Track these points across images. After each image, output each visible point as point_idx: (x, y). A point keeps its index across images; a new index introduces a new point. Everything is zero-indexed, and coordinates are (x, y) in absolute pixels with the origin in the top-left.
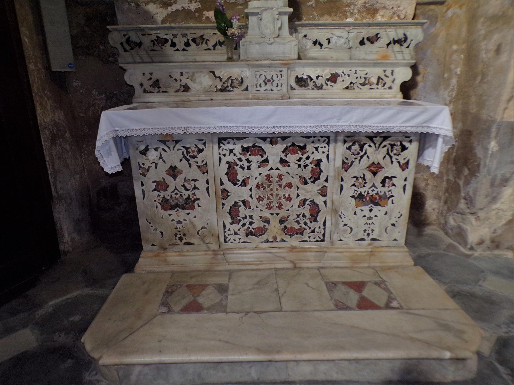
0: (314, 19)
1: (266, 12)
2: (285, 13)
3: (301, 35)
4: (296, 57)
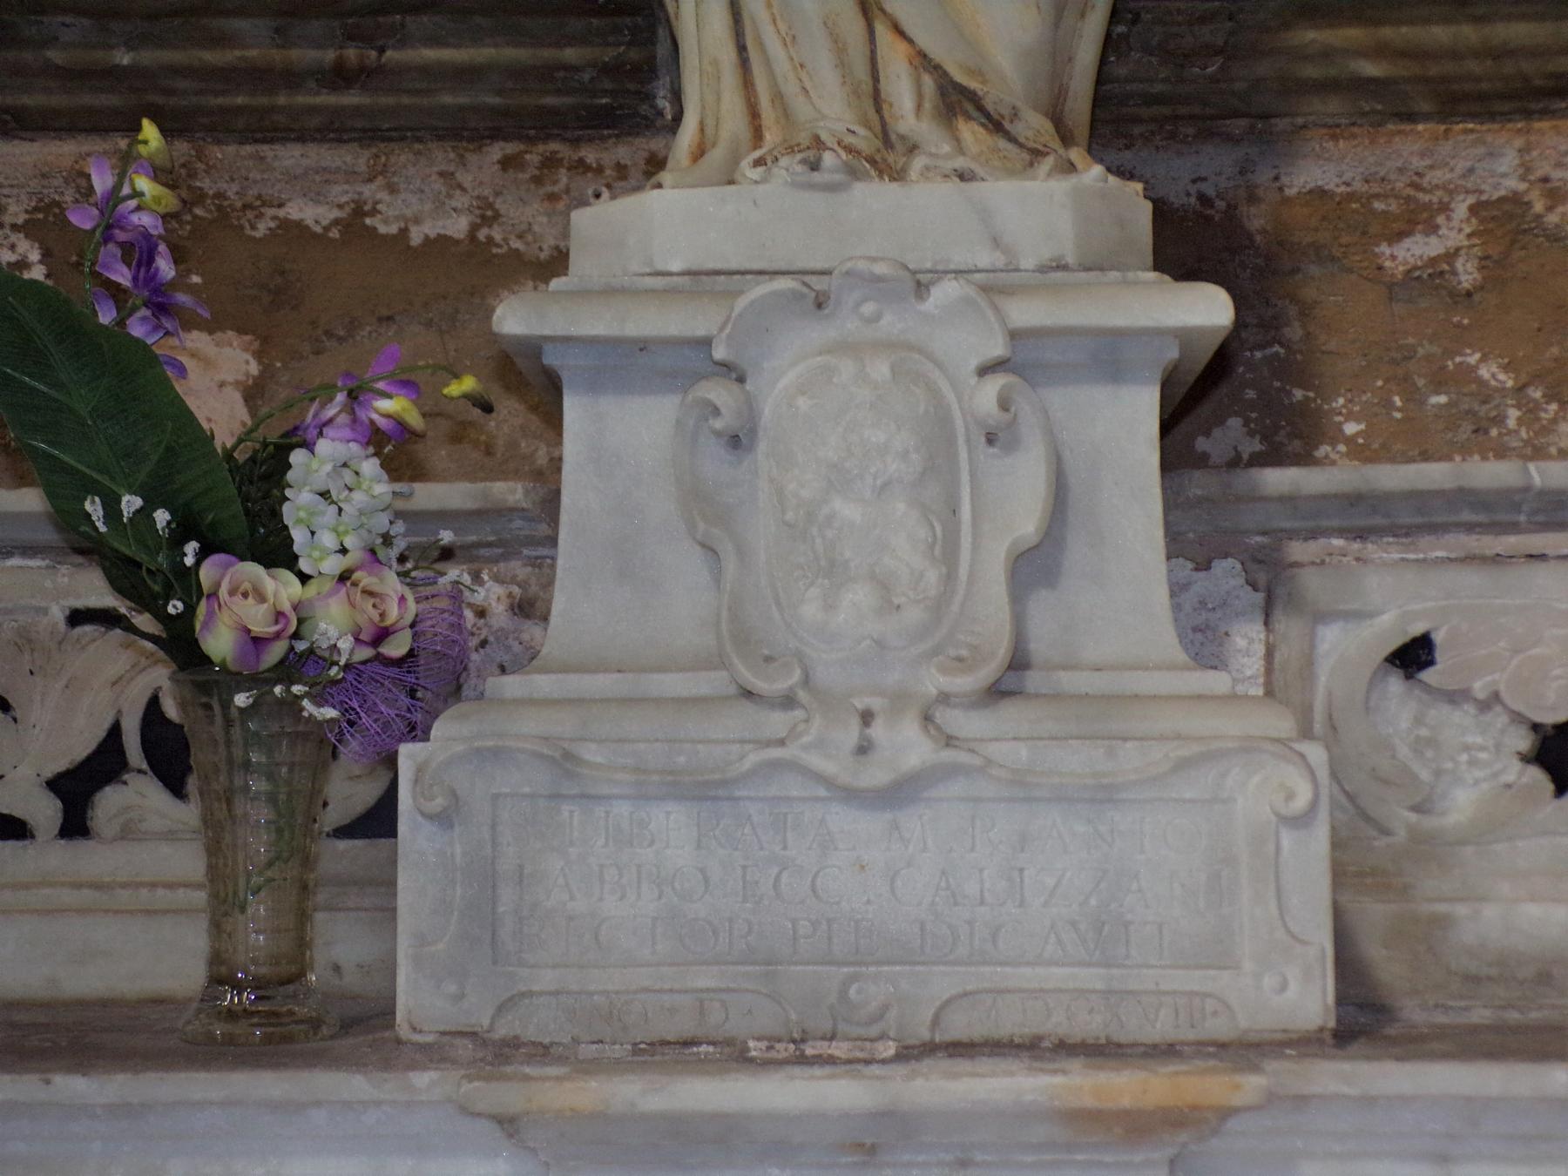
0: (1478, 431)
1: (818, 333)
2: (1107, 355)
3: (1346, 648)
4: (1309, 998)
